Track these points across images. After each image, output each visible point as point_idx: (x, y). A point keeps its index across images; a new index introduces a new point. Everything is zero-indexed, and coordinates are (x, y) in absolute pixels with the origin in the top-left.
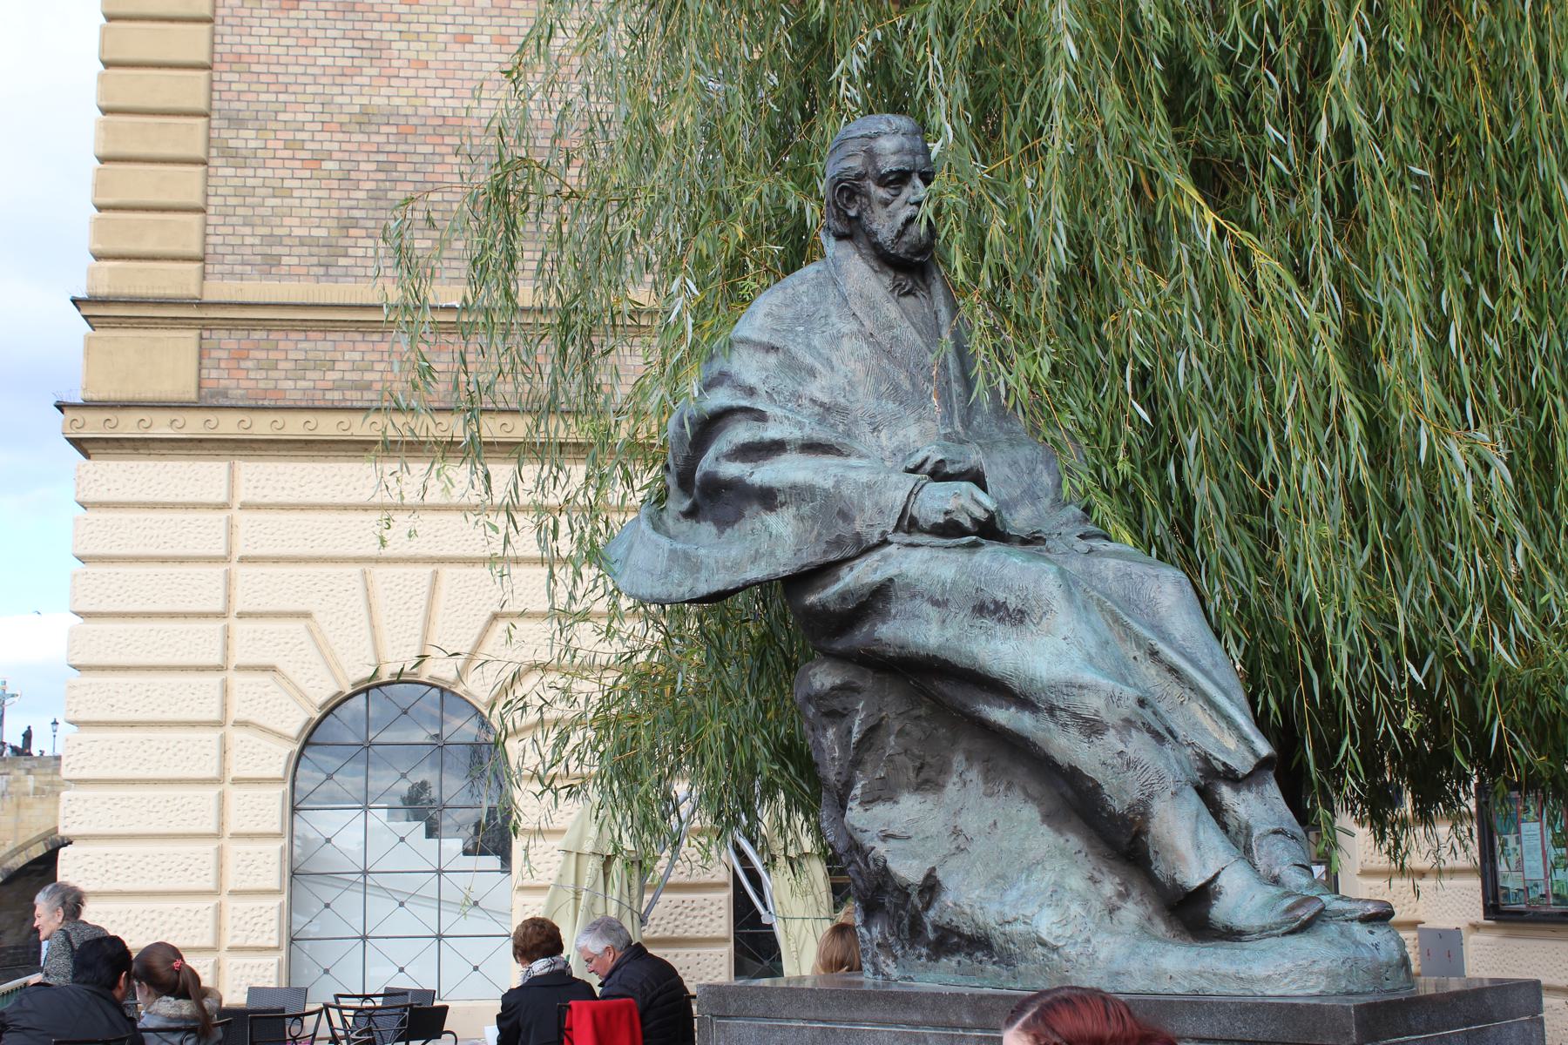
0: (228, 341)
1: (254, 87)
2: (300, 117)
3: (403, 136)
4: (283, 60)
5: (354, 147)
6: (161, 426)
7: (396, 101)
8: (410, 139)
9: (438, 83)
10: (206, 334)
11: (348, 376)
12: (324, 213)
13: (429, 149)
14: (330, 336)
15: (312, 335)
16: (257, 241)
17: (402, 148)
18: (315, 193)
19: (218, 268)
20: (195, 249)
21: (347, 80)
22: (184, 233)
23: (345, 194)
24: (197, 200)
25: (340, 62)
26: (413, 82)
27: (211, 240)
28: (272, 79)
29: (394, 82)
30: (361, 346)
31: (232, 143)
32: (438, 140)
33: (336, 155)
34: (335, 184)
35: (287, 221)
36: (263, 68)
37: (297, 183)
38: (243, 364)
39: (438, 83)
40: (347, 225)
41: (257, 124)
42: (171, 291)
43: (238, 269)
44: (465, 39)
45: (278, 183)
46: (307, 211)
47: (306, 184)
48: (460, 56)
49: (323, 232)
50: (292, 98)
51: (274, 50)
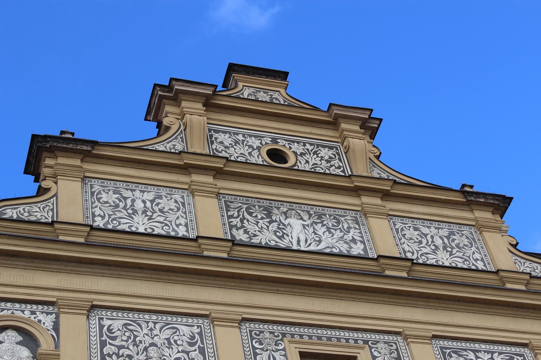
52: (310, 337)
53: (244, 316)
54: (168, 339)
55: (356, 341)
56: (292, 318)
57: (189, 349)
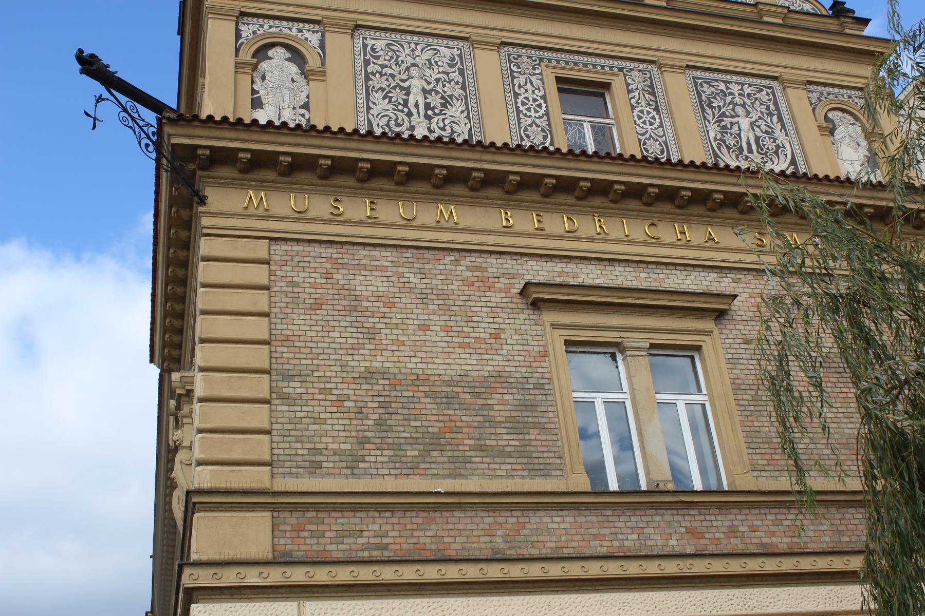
0: (291, 519)
1: (297, 356)
2: (328, 374)
3: (393, 387)
4: (314, 339)
5: (363, 393)
6: (253, 577)
7: (387, 365)
8: (398, 388)
9: (412, 354)
10: (276, 514)
11: (372, 540)
12: (348, 434)
13: (410, 394)
14: (358, 514)
15: (346, 514)
16: (306, 452)
17: (393, 393)
18: (341, 422)
19: (281, 470)
20: (266, 457)
21: (356, 352)
22: (259, 447)
23: (360, 422)
24: (266, 425)
25: (350, 341)
26: (396, 353)
27: (276, 451)
28: (308, 350)
29: (384, 353)
30: (379, 521)
31: (285, 390)
32: (415, 388)
33: (352, 398)
34: (353, 416)
35: (324, 439)
36: (303, 344)
37: (329, 415)
38: (302, 534)
39: (412, 354)
40: (362, 442)
41: (301, 379)
42: (254, 485)
43: (294, 470)
44: (425, 328)
45: (317, 415)
46: (337, 434)
47: (334, 415)
48: (424, 338)
49: (348, 446)
50: (322, 363)
51: (308, 333)
52: (567, 63)
53: (504, 40)
54: (429, 60)
55: (611, 68)
56: (550, 43)
57: (449, 70)
